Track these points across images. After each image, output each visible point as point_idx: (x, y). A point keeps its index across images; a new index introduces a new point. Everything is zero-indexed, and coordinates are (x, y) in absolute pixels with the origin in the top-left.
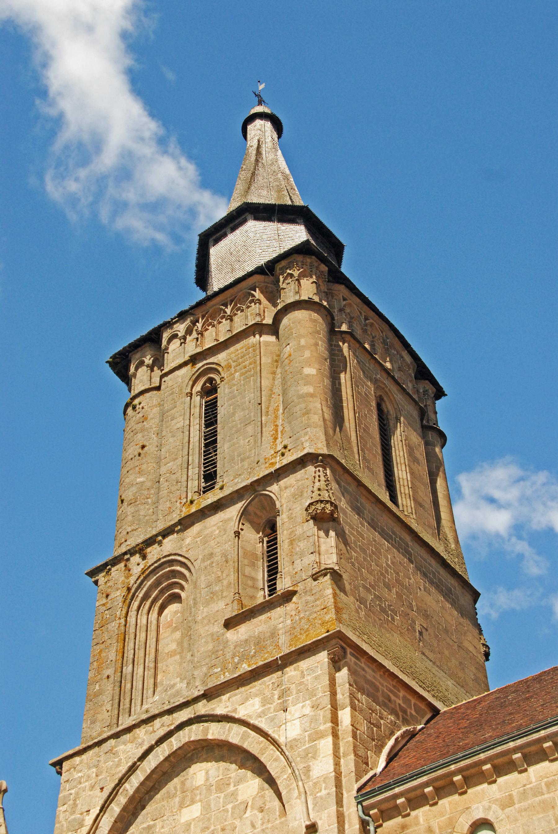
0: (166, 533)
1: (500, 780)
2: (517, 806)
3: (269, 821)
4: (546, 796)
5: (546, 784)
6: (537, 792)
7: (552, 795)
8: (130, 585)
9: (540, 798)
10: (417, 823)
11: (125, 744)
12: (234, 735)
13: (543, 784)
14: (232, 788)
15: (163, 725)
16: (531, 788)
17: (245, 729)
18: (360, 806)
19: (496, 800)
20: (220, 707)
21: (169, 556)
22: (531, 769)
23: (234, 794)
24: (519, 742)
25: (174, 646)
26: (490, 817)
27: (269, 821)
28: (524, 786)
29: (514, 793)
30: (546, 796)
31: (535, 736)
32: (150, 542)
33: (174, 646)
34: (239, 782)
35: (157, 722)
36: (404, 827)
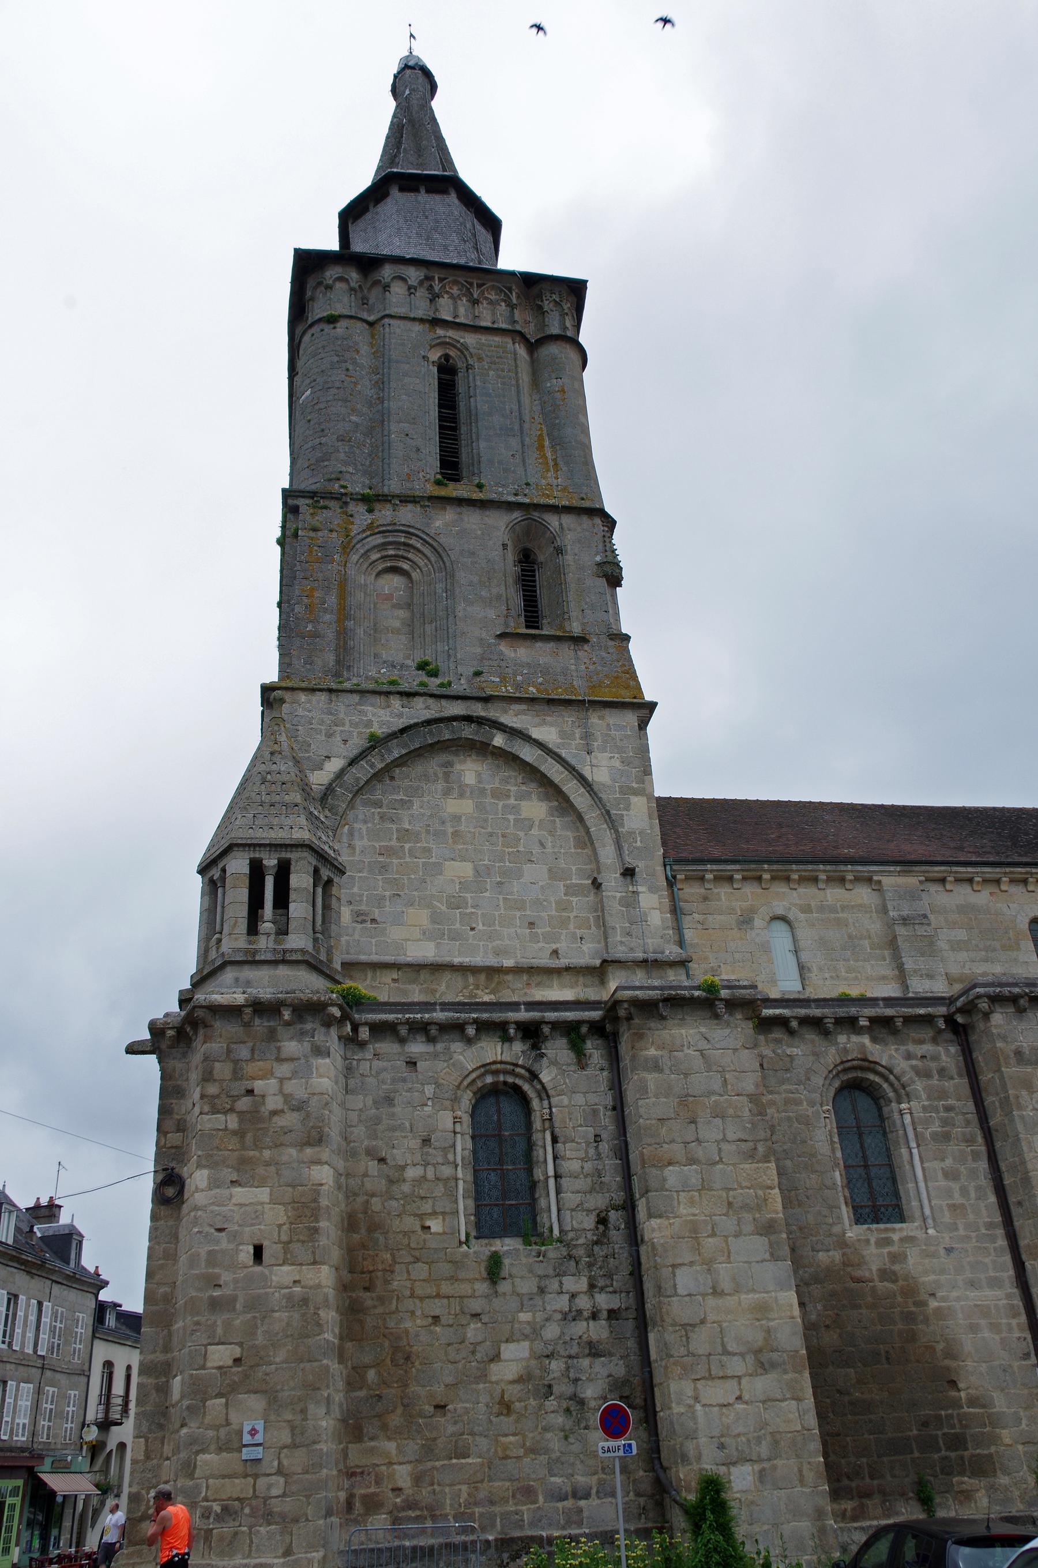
0: (407, 499)
3: (561, 846)
4: (841, 915)
6: (833, 910)
7: (845, 915)
8: (352, 534)
10: (720, 900)
11: (372, 705)
12: (528, 754)
14: (512, 801)
15: (428, 708)
17: (540, 752)
18: (668, 867)
20: (512, 718)
21: (413, 527)
23: (515, 809)
25: (397, 624)
26: (791, 916)
27: (561, 846)
29: (813, 904)
30: (841, 915)
32: (384, 499)
33: (397, 624)
34: (521, 797)
35: (419, 702)
36: (705, 899)
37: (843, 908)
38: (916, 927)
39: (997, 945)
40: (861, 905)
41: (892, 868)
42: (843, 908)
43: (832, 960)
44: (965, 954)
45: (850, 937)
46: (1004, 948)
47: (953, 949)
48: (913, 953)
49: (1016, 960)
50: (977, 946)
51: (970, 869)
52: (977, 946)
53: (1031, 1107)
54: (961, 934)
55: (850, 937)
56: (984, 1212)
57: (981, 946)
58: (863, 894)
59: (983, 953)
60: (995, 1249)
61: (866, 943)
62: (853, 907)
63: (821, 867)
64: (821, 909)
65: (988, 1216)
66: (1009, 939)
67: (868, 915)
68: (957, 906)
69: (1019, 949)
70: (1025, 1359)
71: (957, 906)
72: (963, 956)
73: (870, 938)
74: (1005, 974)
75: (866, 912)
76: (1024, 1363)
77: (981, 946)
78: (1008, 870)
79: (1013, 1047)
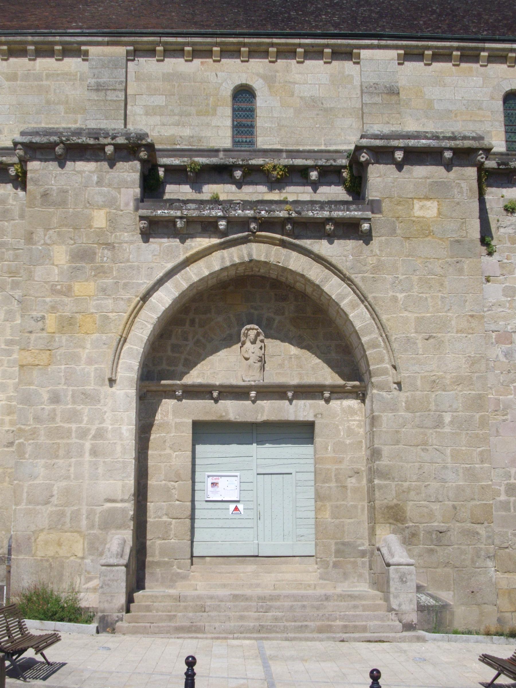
1: (12, 60)
2: (18, 82)
4: (44, 83)
5: (46, 75)
6: (38, 77)
7: (48, 83)
9: (39, 83)
13: (44, 74)
16: (34, 74)
19: (3, 73)
22: (39, 60)
24: (37, 39)
28: (29, 70)
29: (20, 73)
30: (44, 83)
31: (51, 39)
37: (48, 76)
38: (109, 93)
39: (193, 110)
40: (66, 74)
41: (100, 39)
42: (48, 76)
43: (25, 123)
44: (158, 118)
45: (48, 102)
46: (199, 113)
47: (147, 114)
48: (98, 116)
49: (208, 125)
50: (172, 111)
51: (180, 40)
52: (172, 111)
53: (42, 242)
54: (160, 100)
55: (48, 102)
56: (8, 331)
57: (177, 111)
58: (72, 64)
59: (177, 118)
60: (9, 361)
61: (61, 108)
62: (58, 75)
63: (30, 38)
64: (26, 77)
65: (11, 335)
66: (208, 105)
67: (72, 83)
68: (164, 74)
69: (214, 114)
70: (8, 447)
71: (164, 74)
72: (157, 119)
73: (67, 103)
74: (192, 137)
75: (70, 80)
76: (6, 449)
77: (177, 111)
78: (219, 40)
79: (42, 190)
